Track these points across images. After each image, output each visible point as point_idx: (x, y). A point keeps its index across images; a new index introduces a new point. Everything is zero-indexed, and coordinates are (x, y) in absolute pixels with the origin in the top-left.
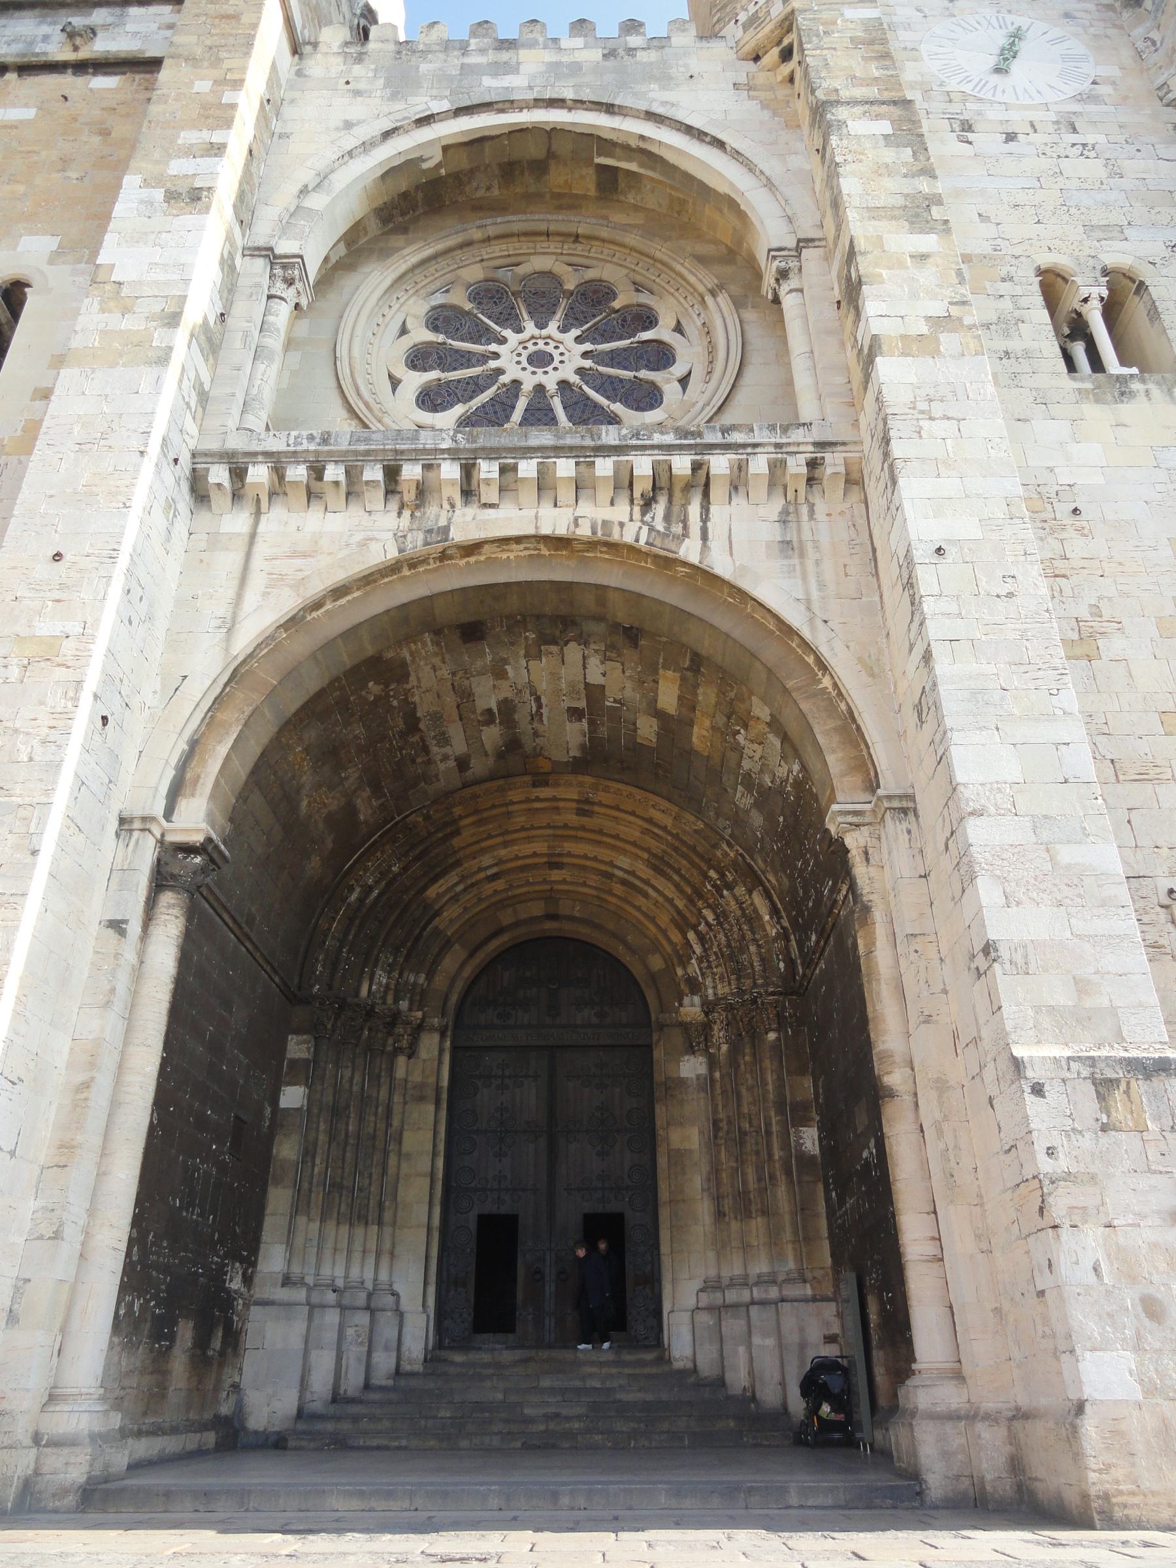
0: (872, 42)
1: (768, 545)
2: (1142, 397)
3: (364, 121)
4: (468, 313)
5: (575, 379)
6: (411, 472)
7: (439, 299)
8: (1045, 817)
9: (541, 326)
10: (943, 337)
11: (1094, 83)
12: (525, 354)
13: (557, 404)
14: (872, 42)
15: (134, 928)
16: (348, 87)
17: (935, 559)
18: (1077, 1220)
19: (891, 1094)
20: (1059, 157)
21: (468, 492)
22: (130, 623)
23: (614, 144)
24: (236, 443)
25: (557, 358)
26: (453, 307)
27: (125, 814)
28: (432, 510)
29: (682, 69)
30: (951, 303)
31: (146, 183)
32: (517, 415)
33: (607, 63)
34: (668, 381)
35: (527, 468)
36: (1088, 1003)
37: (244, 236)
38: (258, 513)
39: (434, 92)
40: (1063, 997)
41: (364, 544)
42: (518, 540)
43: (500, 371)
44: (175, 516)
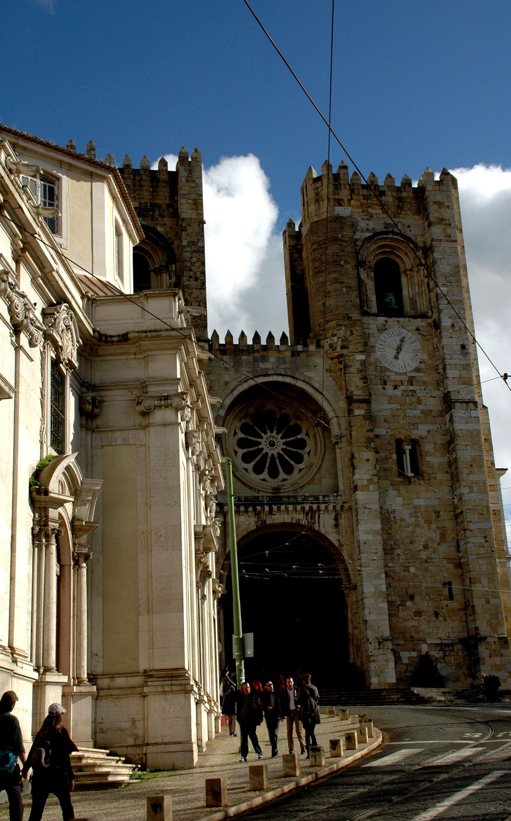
0: (361, 371)
3: (230, 382)
5: (281, 452)
6: (259, 508)
7: (243, 421)
9: (272, 432)
11: (420, 363)
12: (268, 442)
13: (277, 460)
14: (361, 371)
16: (223, 366)
17: (363, 544)
19: (350, 639)
25: (276, 444)
28: (262, 515)
30: (373, 475)
32: (267, 465)
34: (305, 454)
35: (283, 507)
39: (247, 370)
41: (249, 525)
43: (262, 449)
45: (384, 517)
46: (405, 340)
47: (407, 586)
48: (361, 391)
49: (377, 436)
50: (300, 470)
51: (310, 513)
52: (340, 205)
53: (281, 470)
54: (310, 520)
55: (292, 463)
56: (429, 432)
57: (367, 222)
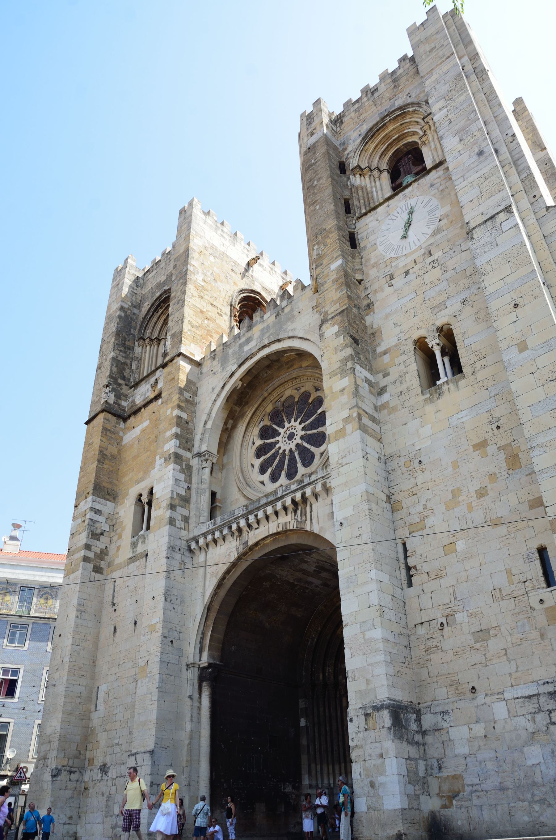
0: (337, 280)
1: (328, 516)
2: (446, 392)
4: (271, 426)
7: (261, 425)
8: (363, 622)
9: (289, 422)
10: (347, 427)
11: (440, 221)
12: (286, 436)
13: (296, 454)
15: (196, 695)
17: (340, 527)
18: (357, 760)
20: (424, 273)
21: (249, 526)
22: (174, 609)
23: (285, 351)
24: (197, 532)
26: (266, 426)
27: (188, 663)
29: (297, 310)
31: (160, 458)
32: (286, 466)
33: (277, 320)
36: (370, 687)
37: (191, 452)
38: (206, 552)
40: (363, 687)
41: (229, 555)
42: (266, 537)
43: (280, 448)
44: (185, 565)
45: (404, 470)
46: (415, 209)
47: (454, 583)
48: (338, 304)
49: (385, 353)
50: (322, 454)
51: (300, 508)
52: (312, 134)
53: (299, 465)
54: (299, 520)
55: (313, 449)
56: (464, 302)
57: (359, 129)
